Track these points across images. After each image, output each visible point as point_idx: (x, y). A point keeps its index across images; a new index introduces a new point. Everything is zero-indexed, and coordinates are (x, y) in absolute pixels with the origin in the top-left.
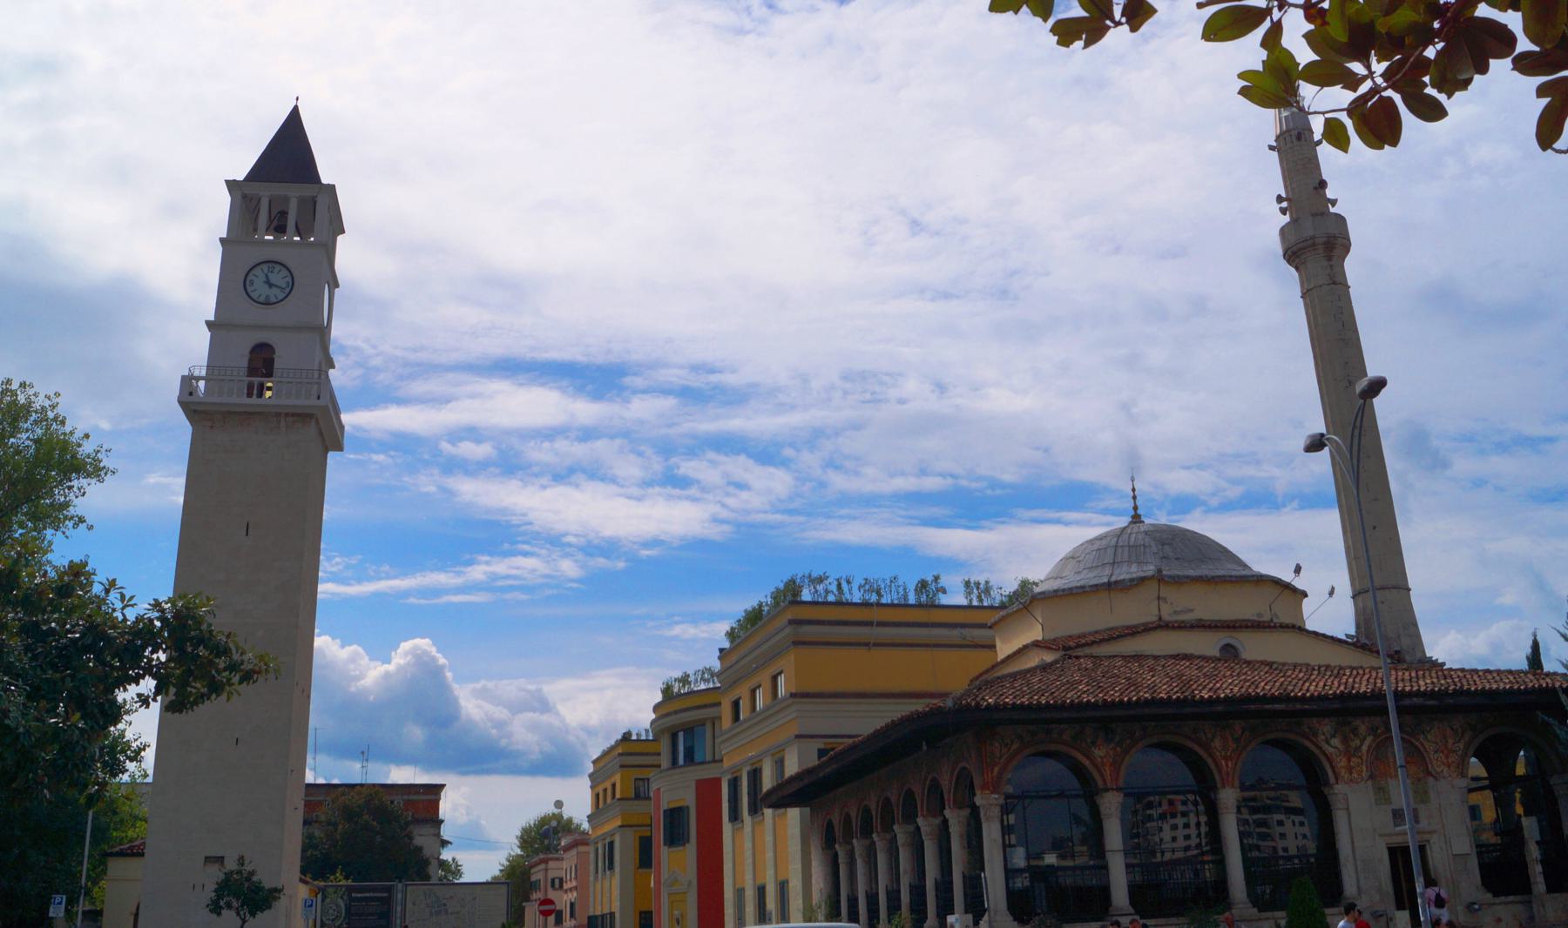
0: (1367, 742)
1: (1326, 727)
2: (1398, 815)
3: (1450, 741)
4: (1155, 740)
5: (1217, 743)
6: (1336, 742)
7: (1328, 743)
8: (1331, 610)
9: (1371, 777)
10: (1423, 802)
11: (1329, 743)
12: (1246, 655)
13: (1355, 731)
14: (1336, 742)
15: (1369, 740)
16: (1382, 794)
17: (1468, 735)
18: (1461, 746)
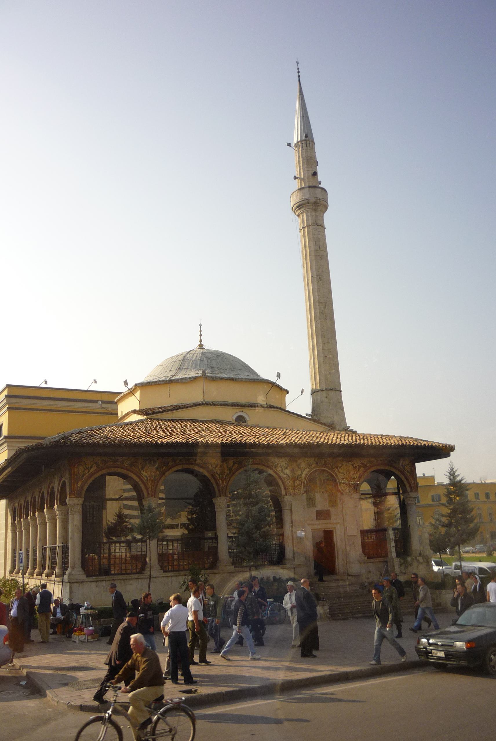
0: (305, 473)
1: (282, 462)
3: (352, 473)
4: (180, 467)
6: (287, 471)
7: (282, 471)
8: (300, 403)
9: (306, 492)
10: (333, 506)
12: (249, 422)
15: (307, 470)
16: (311, 502)
17: (362, 469)
18: (357, 475)
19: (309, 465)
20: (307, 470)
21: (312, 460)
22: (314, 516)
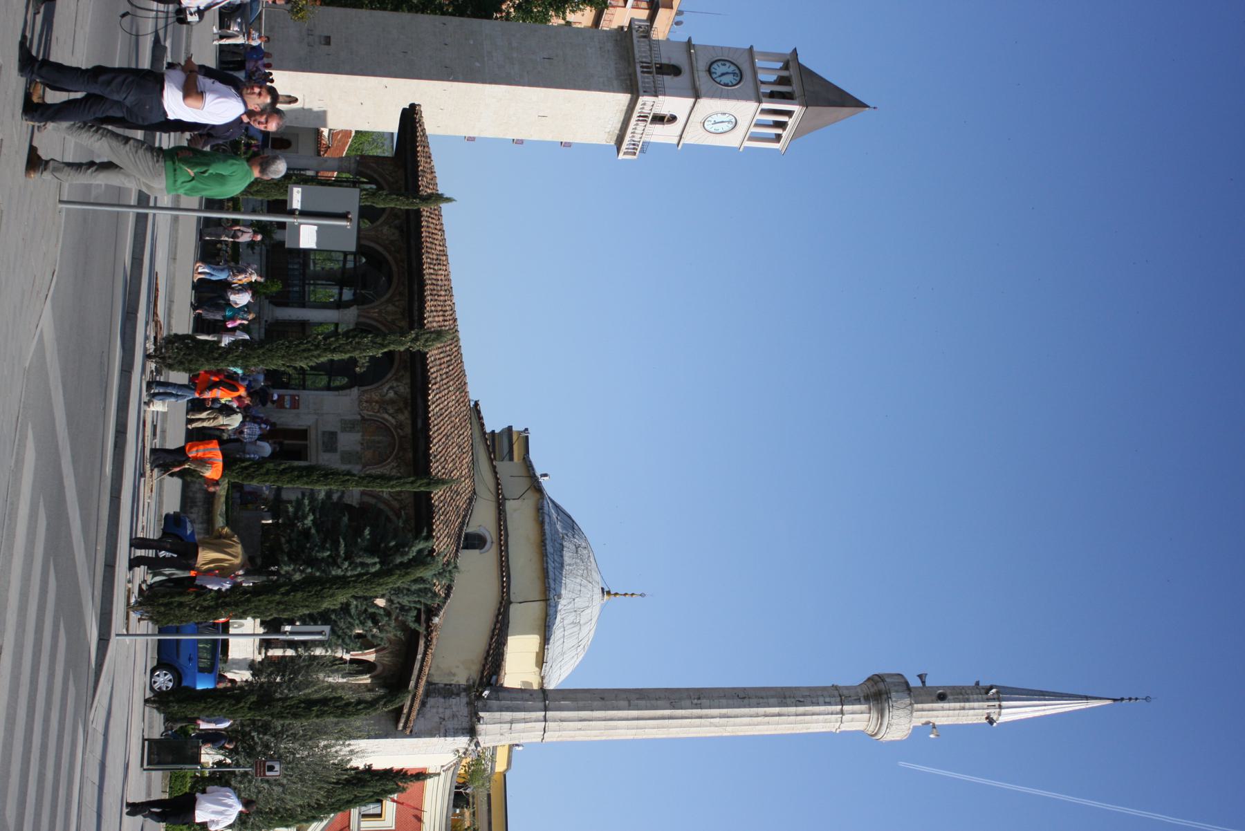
0: (390, 418)
1: (404, 389)
2: (332, 436)
5: (390, 308)
6: (391, 394)
7: (391, 388)
11: (393, 388)
13: (399, 411)
14: (391, 394)
15: (393, 421)
16: (349, 426)
17: (396, 505)
19: (400, 426)
20: (393, 421)
21: (408, 430)
22: (329, 428)
